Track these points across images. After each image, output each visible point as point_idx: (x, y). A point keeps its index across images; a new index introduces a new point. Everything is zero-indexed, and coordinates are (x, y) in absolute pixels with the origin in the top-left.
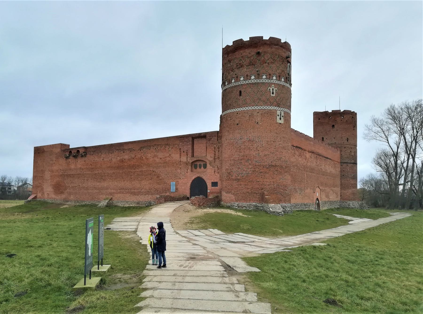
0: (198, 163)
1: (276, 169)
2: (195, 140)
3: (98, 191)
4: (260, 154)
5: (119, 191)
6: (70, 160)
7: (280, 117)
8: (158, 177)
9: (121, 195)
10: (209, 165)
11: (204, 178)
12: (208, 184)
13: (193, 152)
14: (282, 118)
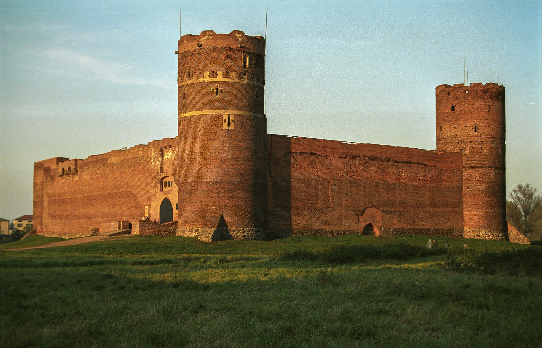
1: (222, 186)
3: (87, 220)
5: (104, 219)
7: (227, 122)
12: (173, 206)
14: (231, 121)
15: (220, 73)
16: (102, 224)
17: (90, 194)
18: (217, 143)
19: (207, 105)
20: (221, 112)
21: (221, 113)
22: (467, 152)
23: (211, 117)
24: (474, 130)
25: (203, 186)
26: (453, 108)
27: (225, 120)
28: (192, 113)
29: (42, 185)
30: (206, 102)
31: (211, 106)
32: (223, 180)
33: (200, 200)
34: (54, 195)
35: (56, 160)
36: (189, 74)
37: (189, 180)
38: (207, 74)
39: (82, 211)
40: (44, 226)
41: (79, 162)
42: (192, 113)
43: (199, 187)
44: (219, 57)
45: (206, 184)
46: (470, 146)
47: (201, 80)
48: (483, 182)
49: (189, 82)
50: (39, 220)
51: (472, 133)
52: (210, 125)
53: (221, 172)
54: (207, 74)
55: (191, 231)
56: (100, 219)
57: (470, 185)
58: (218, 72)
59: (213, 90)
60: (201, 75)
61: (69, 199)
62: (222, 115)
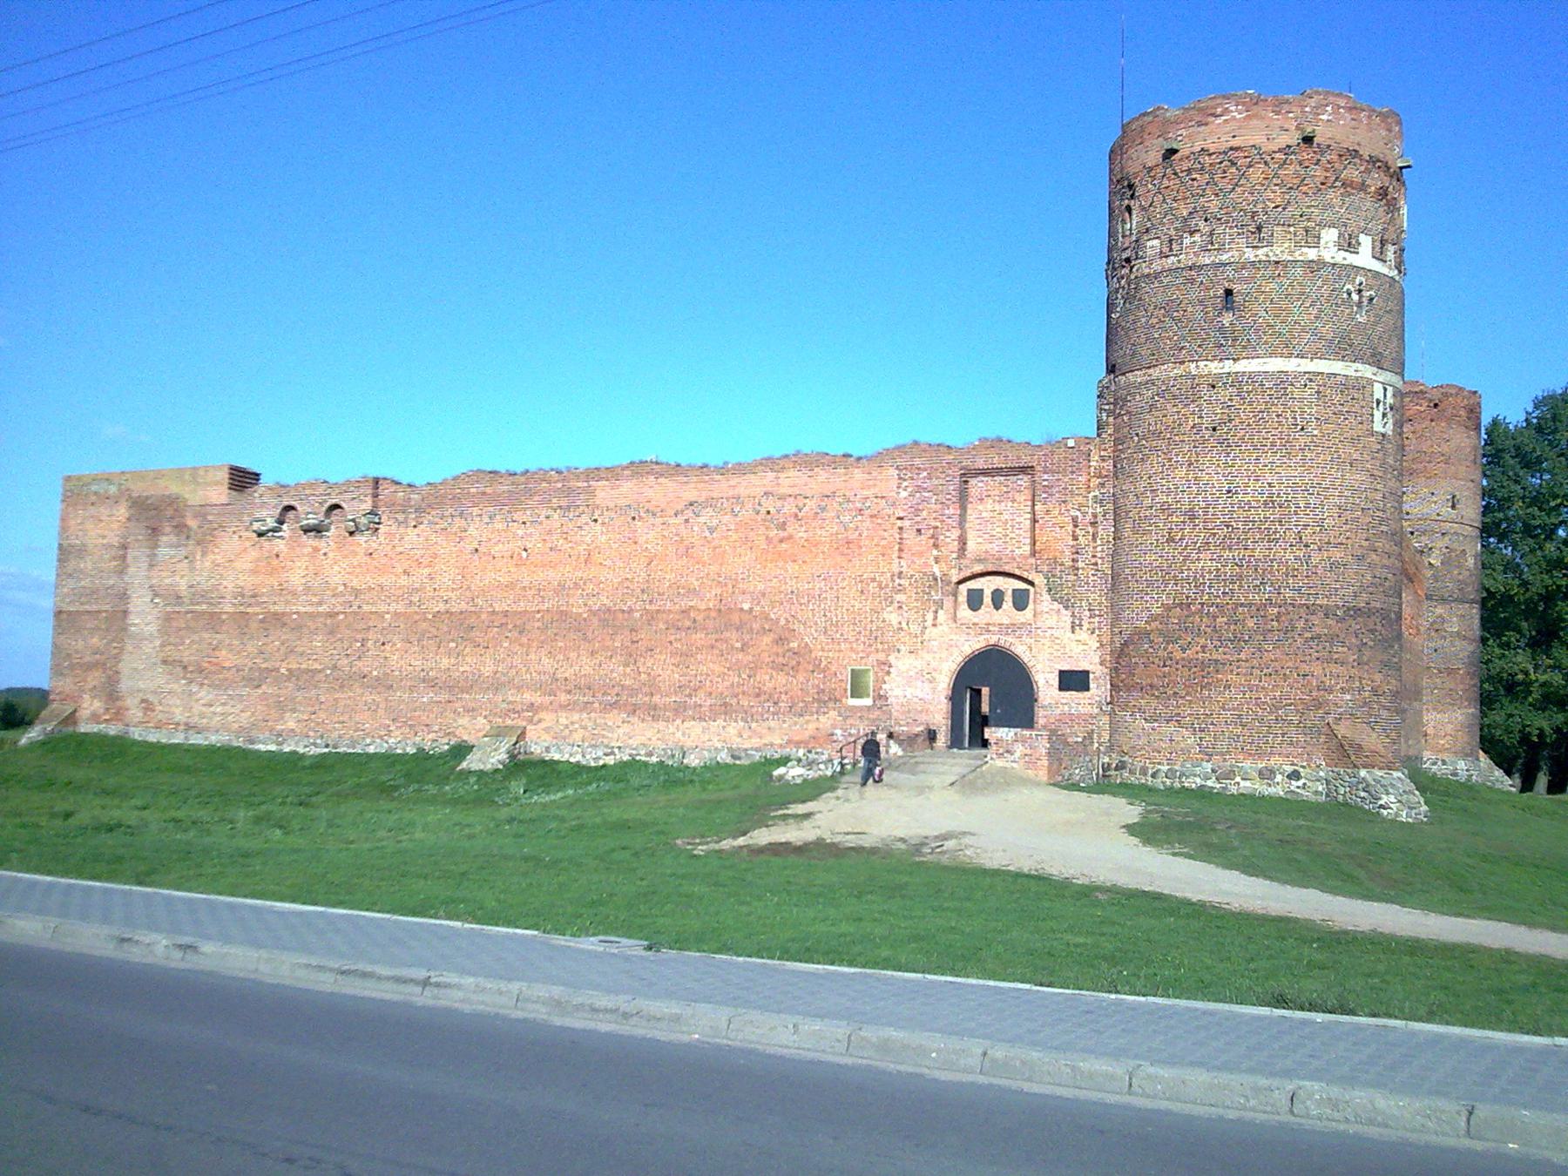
0: (988, 585)
2: (977, 485)
4: (1314, 561)
5: (563, 697)
6: (280, 545)
8: (780, 640)
9: (576, 717)
10: (1046, 597)
11: (1020, 650)
13: (963, 541)
15: (1366, 241)
16: (542, 715)
17: (463, 606)
18: (1357, 478)
20: (1367, 371)
21: (1369, 375)
27: (1378, 402)
28: (1275, 364)
29: (124, 557)
30: (1327, 330)
31: (1342, 348)
32: (1373, 604)
33: (1305, 668)
34: (200, 595)
35: (224, 475)
36: (1259, 229)
38: (1330, 235)
39: (402, 659)
40: (132, 703)
41: (386, 491)
42: (1275, 364)
43: (1300, 624)
44: (1363, 187)
47: (1312, 254)
48: (1465, 638)
49: (1250, 254)
50: (95, 678)
51: (1446, 511)
54: (1330, 235)
55: (1267, 775)
56: (528, 697)
58: (1362, 238)
60: (1311, 237)
61: (312, 615)
62: (1371, 382)
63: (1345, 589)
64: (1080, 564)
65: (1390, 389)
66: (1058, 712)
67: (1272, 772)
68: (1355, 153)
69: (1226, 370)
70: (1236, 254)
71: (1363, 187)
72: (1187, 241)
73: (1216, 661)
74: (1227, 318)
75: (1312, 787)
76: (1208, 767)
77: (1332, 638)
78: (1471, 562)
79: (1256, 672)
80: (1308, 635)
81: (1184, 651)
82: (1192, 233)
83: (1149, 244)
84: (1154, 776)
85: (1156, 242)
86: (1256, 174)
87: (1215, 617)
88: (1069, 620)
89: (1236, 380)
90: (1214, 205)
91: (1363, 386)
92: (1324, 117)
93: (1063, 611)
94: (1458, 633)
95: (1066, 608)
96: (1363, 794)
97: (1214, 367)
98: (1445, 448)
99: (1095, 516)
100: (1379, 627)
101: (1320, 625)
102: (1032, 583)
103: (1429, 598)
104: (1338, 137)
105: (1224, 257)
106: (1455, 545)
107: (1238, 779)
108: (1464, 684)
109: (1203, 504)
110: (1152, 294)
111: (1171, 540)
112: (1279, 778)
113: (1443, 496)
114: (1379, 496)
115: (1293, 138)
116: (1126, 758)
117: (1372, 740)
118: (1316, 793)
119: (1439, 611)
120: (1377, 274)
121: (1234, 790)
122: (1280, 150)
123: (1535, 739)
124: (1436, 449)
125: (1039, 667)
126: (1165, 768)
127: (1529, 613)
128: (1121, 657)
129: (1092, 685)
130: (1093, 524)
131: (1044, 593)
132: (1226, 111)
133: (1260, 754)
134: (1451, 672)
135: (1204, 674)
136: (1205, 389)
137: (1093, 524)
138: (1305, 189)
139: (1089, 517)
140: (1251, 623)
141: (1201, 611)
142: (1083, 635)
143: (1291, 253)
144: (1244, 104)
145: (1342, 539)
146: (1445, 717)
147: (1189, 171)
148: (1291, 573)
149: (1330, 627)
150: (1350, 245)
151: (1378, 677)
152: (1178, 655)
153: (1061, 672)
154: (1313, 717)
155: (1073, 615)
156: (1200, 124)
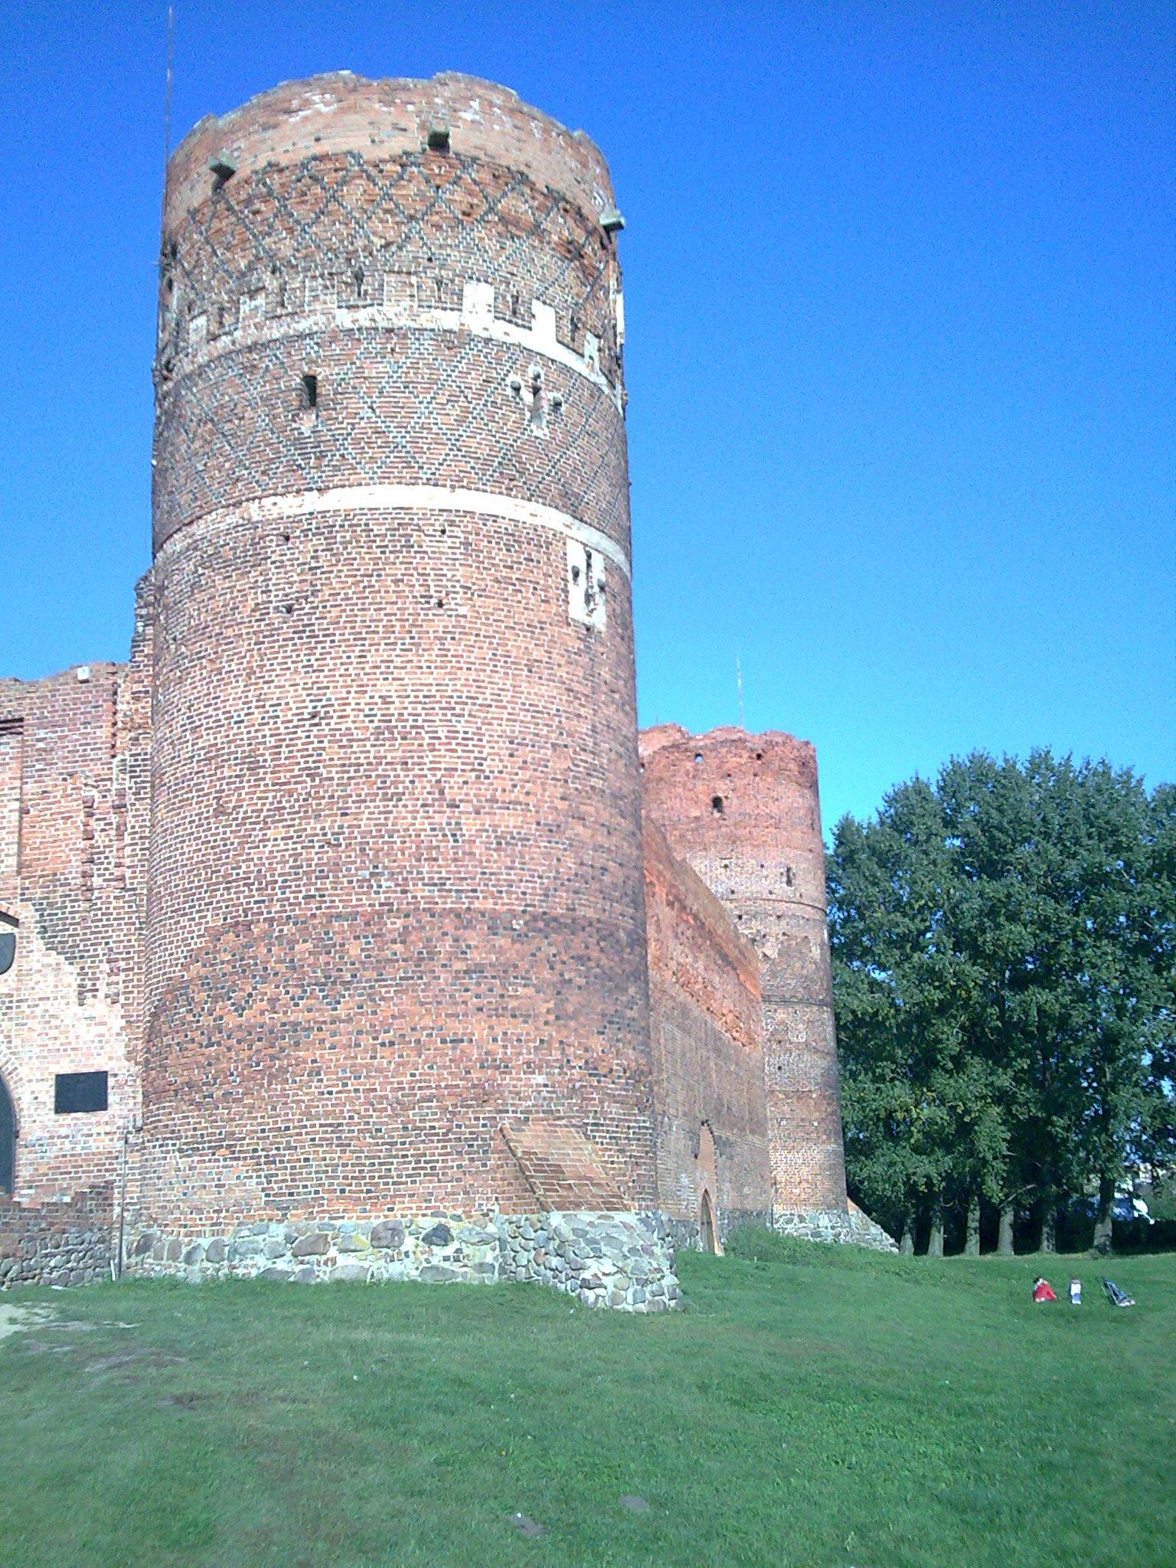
10: (38, 944)
15: (544, 317)
18: (542, 692)
19: (486, 463)
20: (555, 519)
21: (560, 528)
22: (771, 950)
23: (515, 537)
24: (785, 879)
25: (473, 938)
26: (717, 803)
27: (576, 574)
28: (388, 496)
30: (479, 444)
31: (508, 473)
32: (581, 912)
33: (456, 1027)
36: (359, 277)
37: (365, 903)
42: (388, 496)
44: (536, 230)
45: (493, 930)
46: (776, 929)
47: (449, 320)
48: (817, 1051)
49: (344, 319)
51: (781, 888)
52: (508, 581)
53: (570, 862)
55: (386, 1238)
57: (784, 1058)
58: (537, 306)
59: (517, 389)
60: (448, 293)
63: (525, 882)
64: (97, 881)
65: (598, 561)
66: (54, 1151)
67: (396, 1231)
68: (524, 179)
69: (306, 510)
70: (323, 319)
71: (536, 230)
72: (245, 308)
73: (296, 1025)
74: (307, 423)
75: (473, 1257)
76: (278, 1231)
77: (505, 971)
78: (816, 952)
79: (367, 1040)
80: (459, 966)
81: (240, 1010)
82: (252, 294)
83: (192, 326)
84: (189, 1259)
85: (201, 321)
86: (354, 194)
87: (292, 944)
88: (74, 981)
89: (323, 526)
90: (286, 248)
91: (546, 542)
92: (468, 116)
93: (67, 967)
94: (807, 1044)
95: (71, 959)
96: (555, 1261)
97: (289, 506)
98: (774, 809)
99: (121, 794)
100: (594, 953)
101: (480, 948)
102: (15, 922)
103: (767, 999)
104: (491, 148)
105: (303, 325)
106: (794, 931)
107: (333, 1252)
108: (817, 1112)
109: (272, 741)
110: (197, 401)
111: (220, 811)
112: (409, 1243)
113: (774, 870)
114: (584, 728)
115: (415, 141)
116: (155, 1230)
117: (583, 1156)
118: (481, 1267)
119: (781, 1015)
120: (566, 370)
121: (324, 1275)
122: (393, 160)
123: (922, 1188)
124: (763, 810)
125: (23, 1071)
126: (205, 1242)
127: (902, 1039)
128: (155, 1035)
129: (111, 1099)
130: (119, 808)
131: (34, 936)
132: (307, 104)
133: (373, 1198)
134: (800, 1096)
135: (274, 1050)
136: (273, 542)
137: (119, 808)
138: (436, 218)
139: (112, 798)
140: (354, 950)
141: (267, 935)
142: (98, 1007)
143: (414, 316)
144: (334, 91)
145: (517, 794)
146: (798, 1158)
147: (248, 202)
148: (424, 854)
149: (501, 951)
150: (515, 311)
151: (597, 1043)
152: (231, 1021)
153: (58, 1076)
154: (472, 1120)
155: (82, 972)
156: (266, 128)
